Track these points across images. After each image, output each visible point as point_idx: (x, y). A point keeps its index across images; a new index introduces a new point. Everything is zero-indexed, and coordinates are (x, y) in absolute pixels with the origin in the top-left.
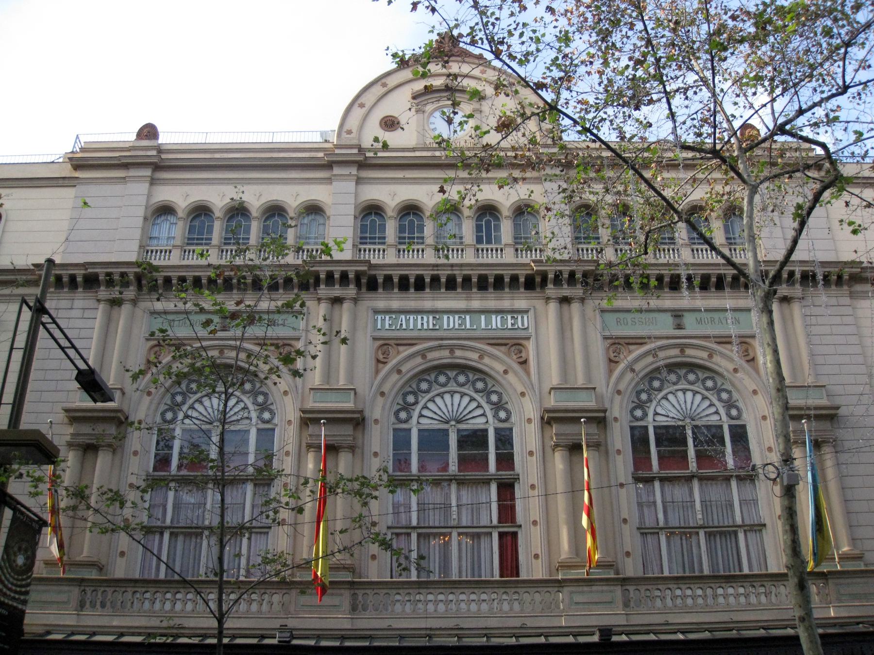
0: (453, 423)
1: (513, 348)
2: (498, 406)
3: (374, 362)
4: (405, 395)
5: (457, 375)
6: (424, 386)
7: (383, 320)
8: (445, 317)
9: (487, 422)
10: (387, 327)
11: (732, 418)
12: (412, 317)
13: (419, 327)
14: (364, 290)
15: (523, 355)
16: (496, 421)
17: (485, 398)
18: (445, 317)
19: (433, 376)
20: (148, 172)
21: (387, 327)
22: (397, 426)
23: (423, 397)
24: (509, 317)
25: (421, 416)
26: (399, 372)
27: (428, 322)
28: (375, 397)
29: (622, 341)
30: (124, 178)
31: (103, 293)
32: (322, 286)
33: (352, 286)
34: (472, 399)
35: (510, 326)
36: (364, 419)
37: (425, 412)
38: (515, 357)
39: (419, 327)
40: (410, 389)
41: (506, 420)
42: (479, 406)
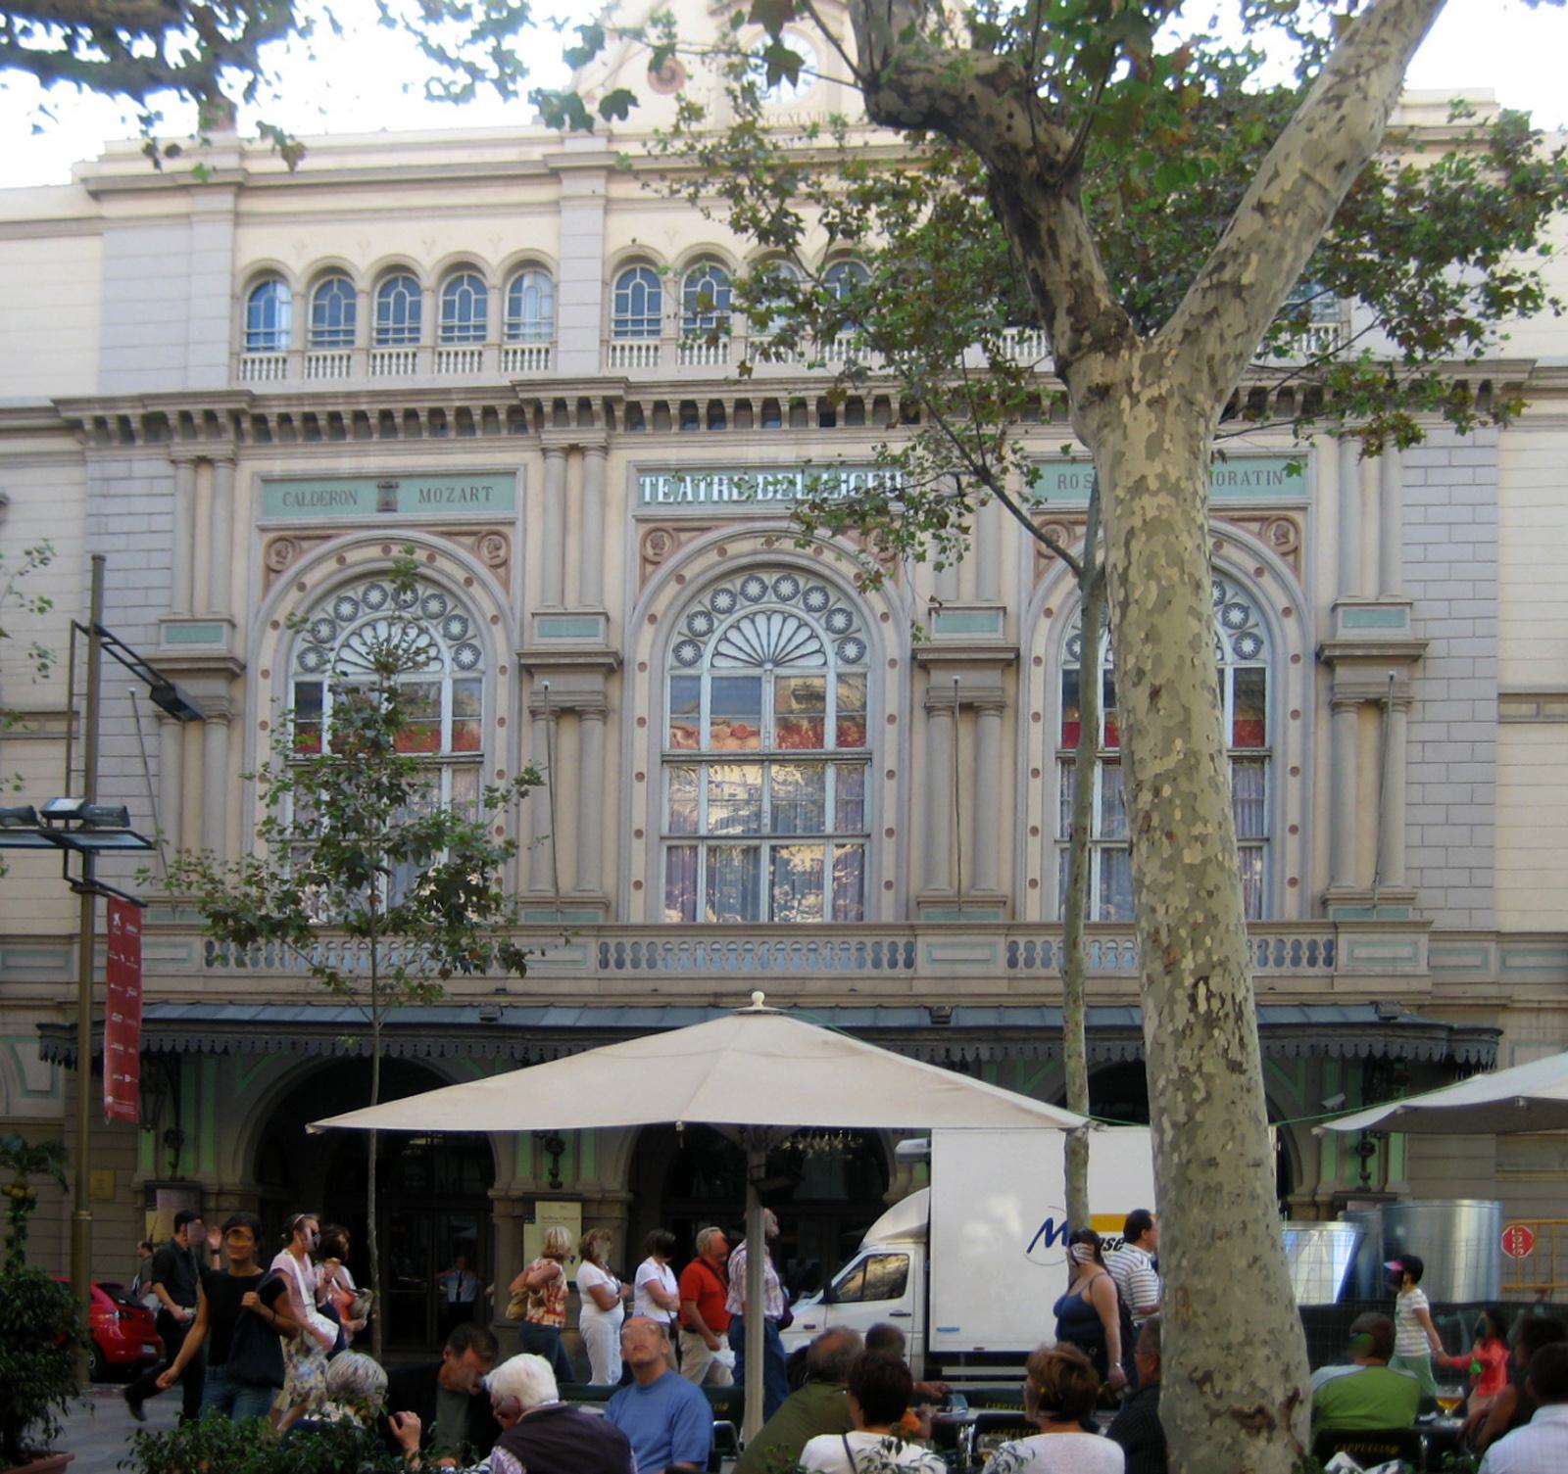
0: (769, 666)
2: (844, 636)
3: (638, 561)
4: (691, 618)
5: (778, 581)
6: (723, 601)
7: (654, 486)
10: (661, 498)
11: (1244, 657)
13: (716, 497)
14: (620, 429)
17: (823, 621)
19: (738, 582)
20: (224, 201)
21: (661, 498)
22: (677, 672)
23: (721, 622)
25: (717, 653)
32: (548, 426)
33: (600, 424)
34: (802, 624)
36: (621, 663)
37: (724, 648)
42: (813, 636)
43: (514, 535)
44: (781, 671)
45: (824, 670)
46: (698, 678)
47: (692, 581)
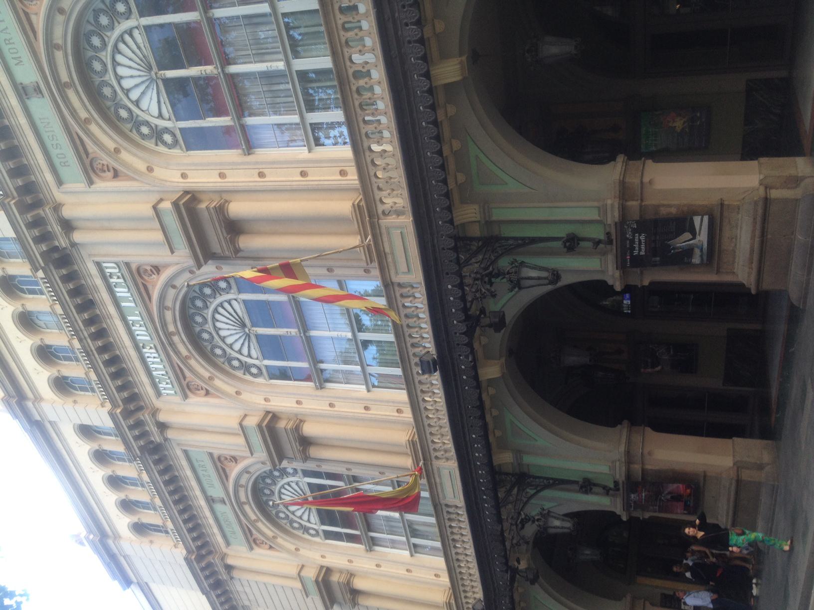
4: (234, 368)
6: (218, 352)
15: (149, 268)
29: (87, 162)
30: (124, 557)
31: (224, 576)
43: (216, 453)
44: (247, 322)
46: (266, 366)
47: (211, 372)
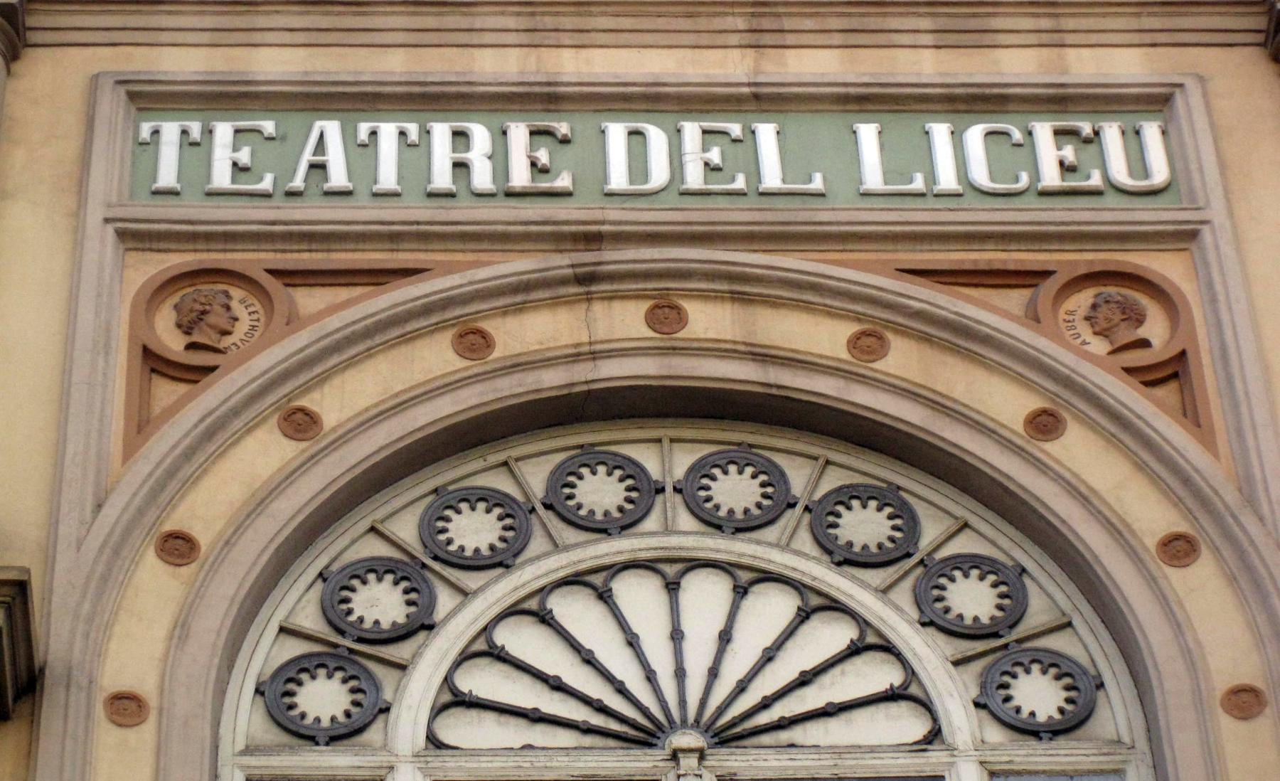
1: (1083, 300)
6: (474, 530)
8: (616, 132)
9: (934, 736)
10: (222, 177)
12: (388, 131)
13: (442, 178)
15: (1155, 328)
16: (995, 734)
17: (903, 595)
18: (616, 132)
24: (1043, 131)
26: (300, 423)
27: (499, 157)
28: (117, 552)
34: (816, 605)
35: (1051, 177)
37: (483, 681)
38: (1099, 347)
39: (442, 178)
40: (379, 549)
41: (1068, 725)
42: (869, 643)
45: (933, 760)
